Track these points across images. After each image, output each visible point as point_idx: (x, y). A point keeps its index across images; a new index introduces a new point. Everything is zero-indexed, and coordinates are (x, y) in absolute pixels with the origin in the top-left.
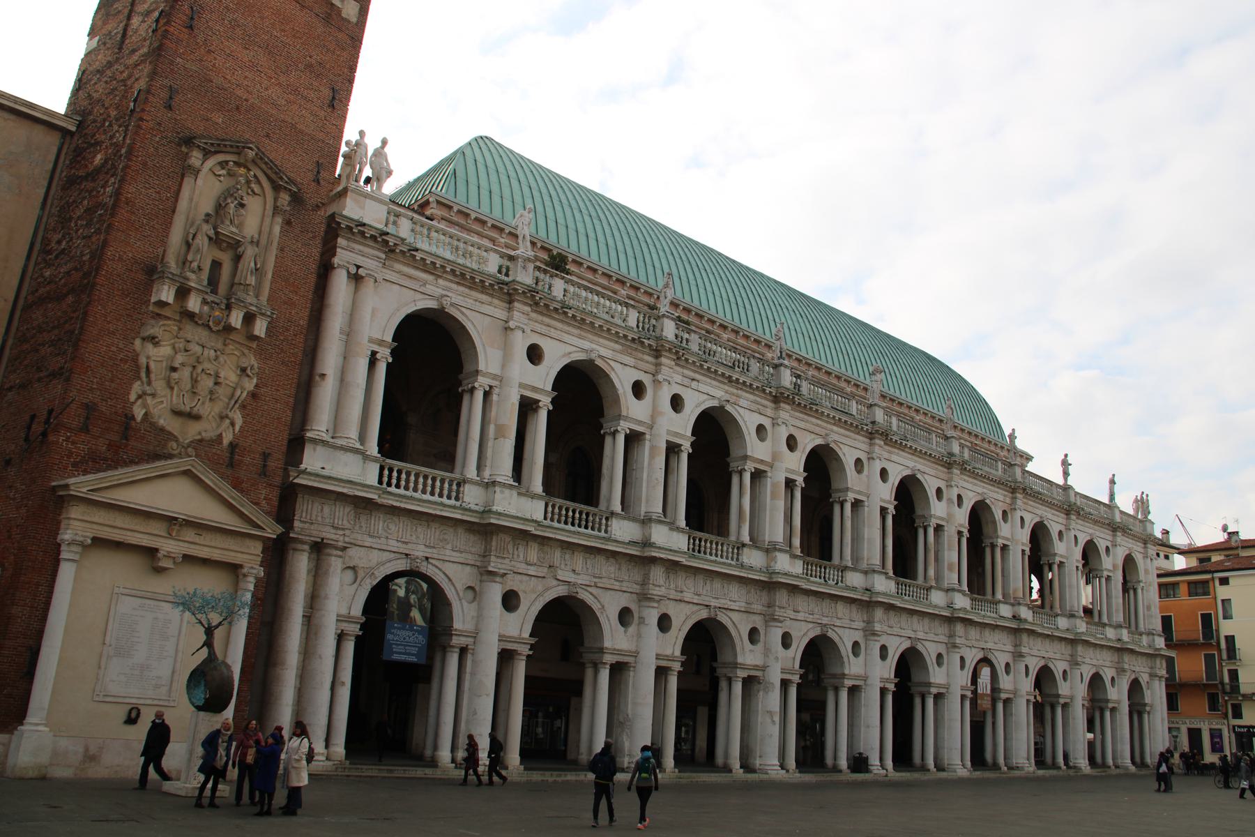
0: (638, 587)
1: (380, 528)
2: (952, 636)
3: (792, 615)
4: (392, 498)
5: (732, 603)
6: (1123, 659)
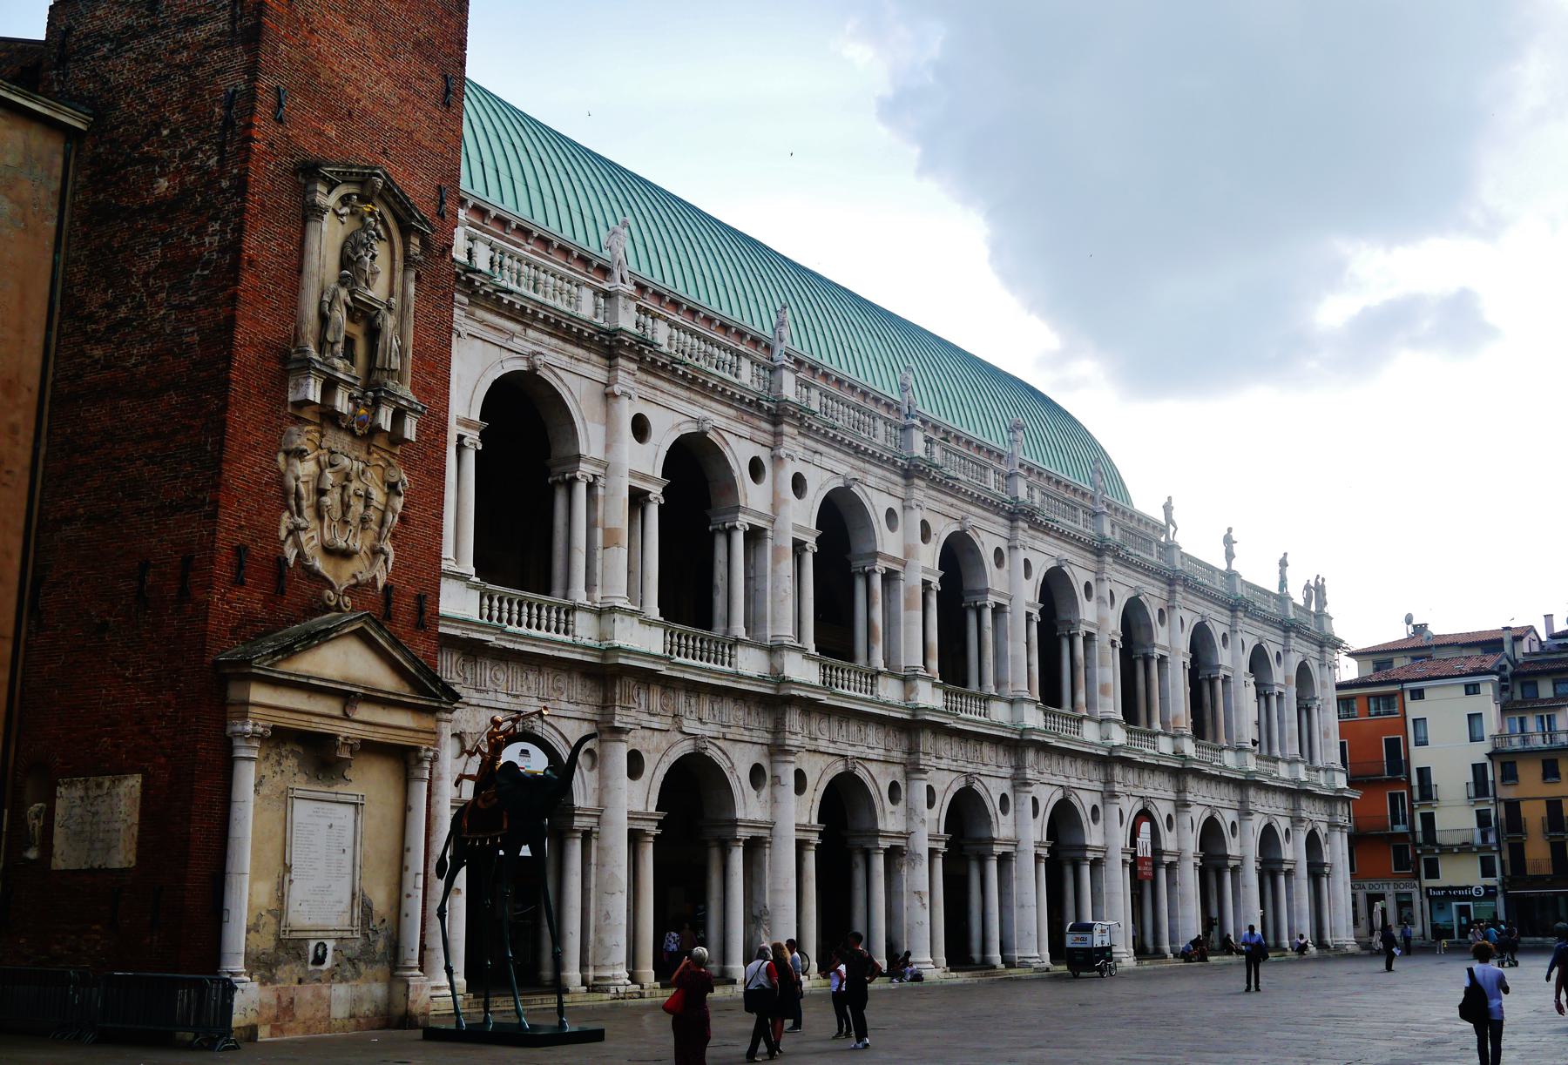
0: (769, 736)
1: (488, 679)
2: (1108, 781)
3: (934, 761)
4: (506, 638)
5: (870, 751)
6: (1300, 805)
